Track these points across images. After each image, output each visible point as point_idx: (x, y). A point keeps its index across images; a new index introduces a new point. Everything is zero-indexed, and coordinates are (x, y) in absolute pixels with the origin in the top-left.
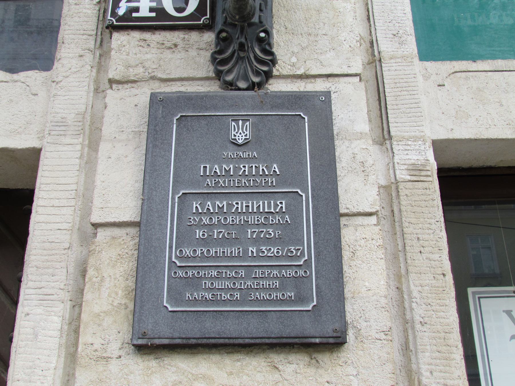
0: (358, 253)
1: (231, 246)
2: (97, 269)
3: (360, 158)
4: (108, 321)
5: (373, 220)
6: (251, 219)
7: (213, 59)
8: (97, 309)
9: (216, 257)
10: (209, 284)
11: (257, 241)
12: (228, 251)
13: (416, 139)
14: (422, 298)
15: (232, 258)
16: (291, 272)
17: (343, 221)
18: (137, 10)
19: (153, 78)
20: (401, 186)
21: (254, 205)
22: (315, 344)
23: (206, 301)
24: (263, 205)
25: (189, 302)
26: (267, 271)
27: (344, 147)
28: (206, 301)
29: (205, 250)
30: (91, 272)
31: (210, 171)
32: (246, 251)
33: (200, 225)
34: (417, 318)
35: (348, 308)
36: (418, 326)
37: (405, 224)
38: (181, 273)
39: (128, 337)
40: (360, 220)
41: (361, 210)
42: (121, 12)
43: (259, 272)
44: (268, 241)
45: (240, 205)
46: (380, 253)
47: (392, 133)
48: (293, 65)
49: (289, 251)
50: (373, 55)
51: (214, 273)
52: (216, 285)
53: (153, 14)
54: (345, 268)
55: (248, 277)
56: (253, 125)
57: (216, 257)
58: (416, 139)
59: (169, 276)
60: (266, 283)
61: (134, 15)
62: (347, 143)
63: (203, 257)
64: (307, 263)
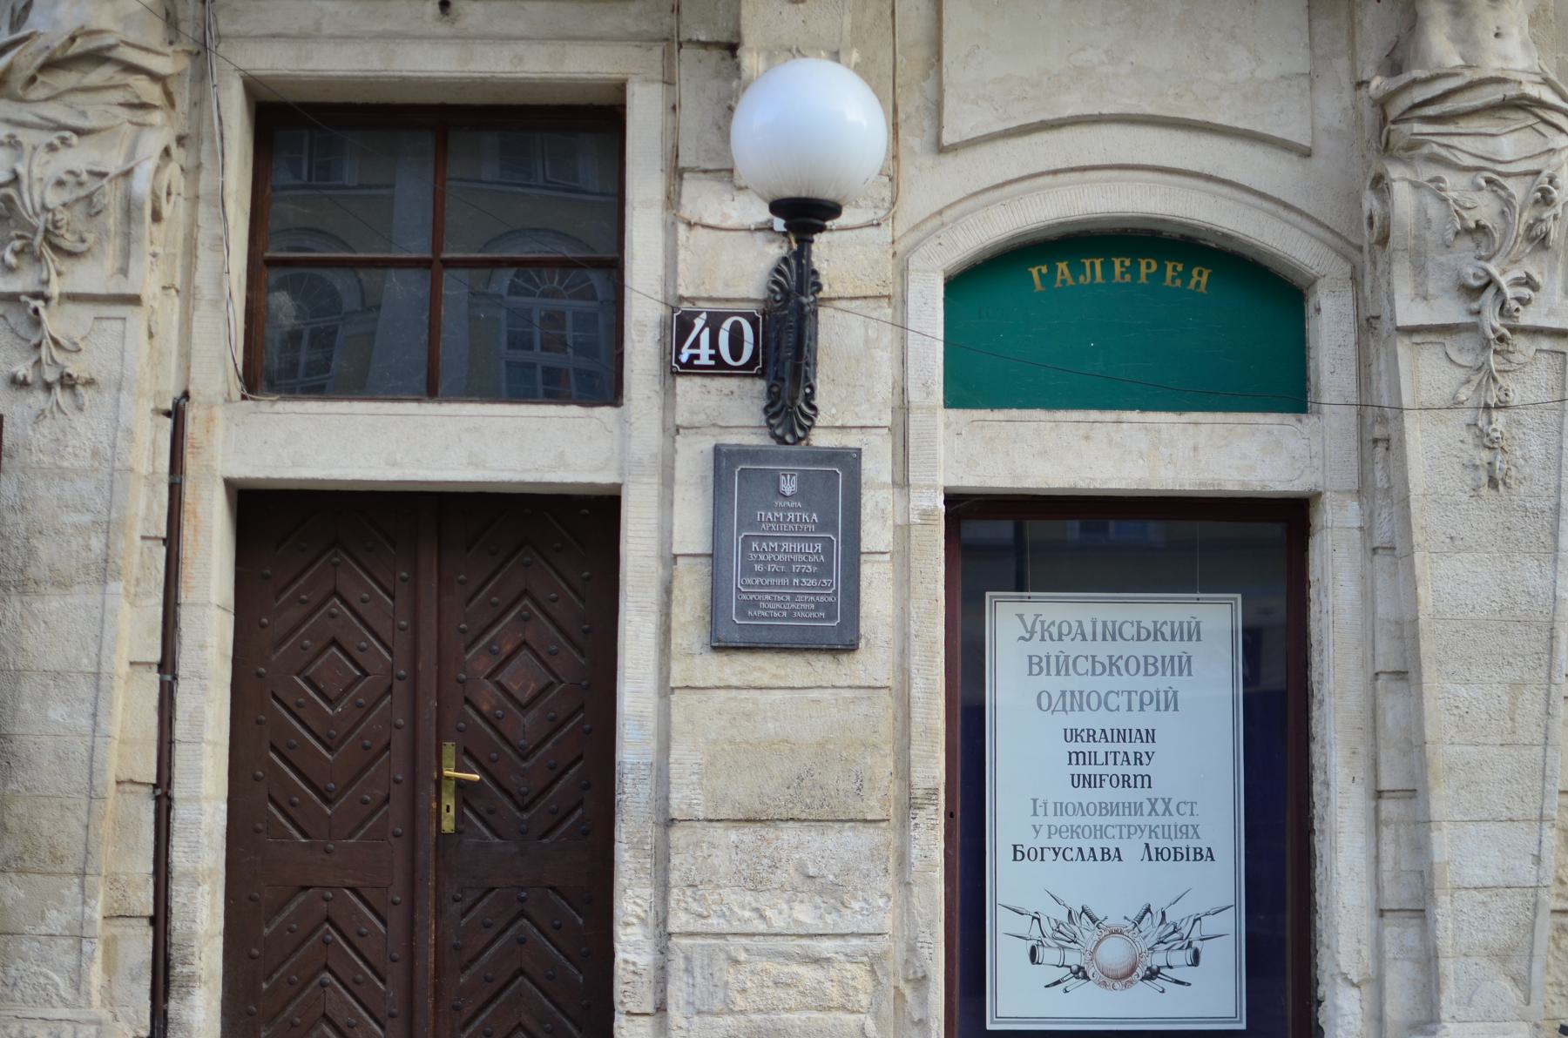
0: (874, 584)
1: (781, 577)
2: (681, 590)
3: (881, 505)
4: (691, 629)
5: (887, 557)
6: (795, 558)
7: (766, 410)
8: (682, 619)
9: (769, 586)
10: (764, 606)
11: (800, 574)
12: (778, 581)
13: (929, 487)
14: (918, 617)
15: (781, 587)
16: (822, 599)
17: (863, 558)
18: (697, 357)
19: (714, 425)
20: (913, 529)
21: (798, 546)
22: (838, 649)
23: (763, 618)
24: (804, 546)
25: (750, 618)
26: (806, 597)
27: (869, 496)
28: (763, 618)
29: (761, 580)
30: (676, 592)
31: (765, 518)
32: (791, 582)
33: (758, 561)
34: (913, 632)
35: (862, 624)
36: (913, 637)
37: (912, 560)
38: (744, 597)
39: (706, 640)
40: (877, 557)
41: (878, 549)
42: (684, 358)
43: (800, 598)
44: (807, 575)
45: (786, 546)
46: (889, 585)
47: (911, 482)
48: (833, 416)
49: (822, 583)
50: (903, 401)
51: (768, 597)
52: (769, 606)
53: (712, 363)
54: (862, 595)
55: (792, 600)
56: (799, 479)
57: (769, 586)
58: (929, 487)
59: (737, 599)
60: (805, 606)
61: (696, 362)
62: (872, 492)
63: (760, 586)
64: (836, 592)
